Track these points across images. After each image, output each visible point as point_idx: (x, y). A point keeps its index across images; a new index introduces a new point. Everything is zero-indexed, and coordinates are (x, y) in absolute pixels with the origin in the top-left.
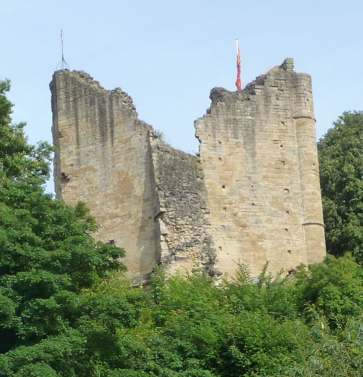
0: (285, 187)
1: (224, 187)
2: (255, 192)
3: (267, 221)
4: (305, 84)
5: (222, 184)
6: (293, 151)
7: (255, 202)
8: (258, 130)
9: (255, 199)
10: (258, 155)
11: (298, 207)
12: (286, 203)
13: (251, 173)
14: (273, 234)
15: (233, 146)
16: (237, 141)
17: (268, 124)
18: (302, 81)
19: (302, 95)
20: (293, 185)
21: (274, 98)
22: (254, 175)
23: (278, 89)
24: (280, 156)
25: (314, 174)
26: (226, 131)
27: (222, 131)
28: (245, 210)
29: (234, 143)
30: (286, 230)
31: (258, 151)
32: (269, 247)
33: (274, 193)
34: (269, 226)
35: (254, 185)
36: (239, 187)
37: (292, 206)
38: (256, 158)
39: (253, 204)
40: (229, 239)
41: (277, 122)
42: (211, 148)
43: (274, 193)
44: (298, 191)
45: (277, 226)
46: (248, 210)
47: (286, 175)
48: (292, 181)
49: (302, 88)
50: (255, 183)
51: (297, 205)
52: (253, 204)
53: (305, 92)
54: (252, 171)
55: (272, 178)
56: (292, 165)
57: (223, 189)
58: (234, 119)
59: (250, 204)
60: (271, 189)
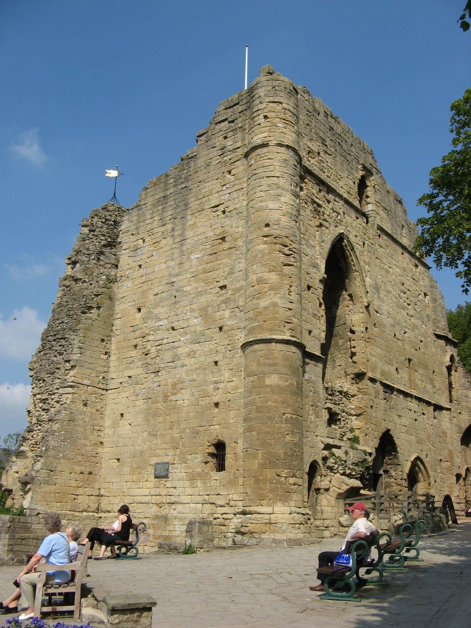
0: (221, 284)
1: (139, 310)
2: (177, 306)
3: (189, 355)
4: (262, 94)
5: (137, 306)
6: (238, 214)
7: (175, 325)
8: (193, 199)
9: (176, 318)
10: (188, 241)
11: (238, 314)
12: (220, 313)
13: (177, 275)
14: (195, 377)
15: (158, 240)
16: (163, 229)
17: (207, 185)
18: (258, 91)
19: (255, 114)
20: (233, 276)
21: (221, 138)
22: (180, 278)
23: (230, 122)
24: (218, 231)
25: (265, 243)
26: (151, 221)
27: (147, 222)
28: (160, 342)
29: (160, 234)
30: (216, 363)
31: (189, 234)
32: (186, 402)
33: (203, 299)
34: (190, 362)
35: (177, 294)
36: (157, 305)
37: (227, 316)
38: (184, 248)
39: (173, 329)
40: (134, 398)
41: (220, 176)
42: (131, 254)
43: (203, 299)
44: (238, 285)
45: (202, 359)
46: (165, 341)
47: (224, 261)
48: (232, 269)
49: (257, 101)
50: (177, 291)
51: (237, 310)
52: (173, 329)
53: (261, 106)
54: (177, 271)
55: (205, 272)
56: (236, 240)
57: (139, 315)
58: (164, 197)
59: (168, 330)
60: (200, 294)
